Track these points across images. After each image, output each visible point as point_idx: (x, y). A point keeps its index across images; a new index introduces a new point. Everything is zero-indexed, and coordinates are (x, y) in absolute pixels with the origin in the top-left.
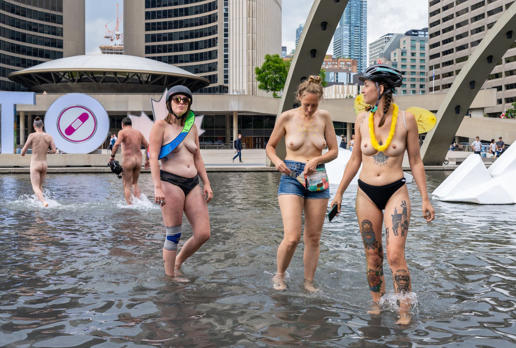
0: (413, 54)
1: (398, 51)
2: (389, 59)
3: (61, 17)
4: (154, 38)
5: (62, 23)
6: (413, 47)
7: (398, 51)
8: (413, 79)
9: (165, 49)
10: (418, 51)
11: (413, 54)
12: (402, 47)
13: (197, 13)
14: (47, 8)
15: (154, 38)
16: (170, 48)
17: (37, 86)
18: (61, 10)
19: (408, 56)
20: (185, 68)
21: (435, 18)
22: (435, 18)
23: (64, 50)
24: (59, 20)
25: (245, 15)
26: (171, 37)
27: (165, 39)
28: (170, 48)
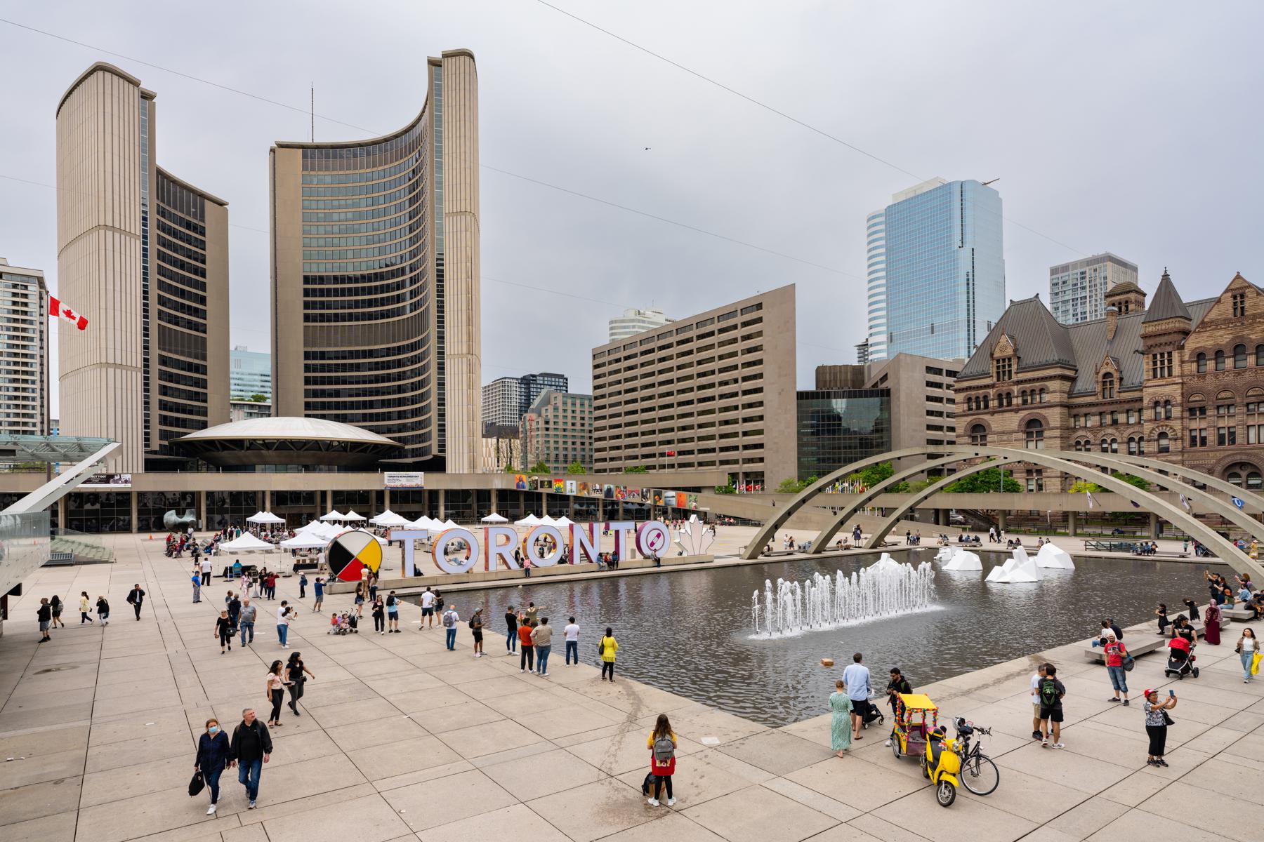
0: (565, 411)
1: (550, 408)
2: (540, 415)
3: (205, 367)
4: (315, 394)
5: (205, 374)
6: (565, 403)
7: (550, 408)
8: (565, 436)
9: (324, 406)
10: (569, 408)
11: (565, 411)
12: (553, 402)
13: (370, 370)
14: (189, 356)
15: (315, 394)
16: (337, 406)
17: (216, 453)
18: (205, 359)
19: (561, 413)
20: (371, 429)
21: (600, 381)
22: (600, 381)
23: (213, 404)
24: (202, 370)
25: (465, 387)
26: (337, 393)
27: (330, 395)
28: (337, 406)
